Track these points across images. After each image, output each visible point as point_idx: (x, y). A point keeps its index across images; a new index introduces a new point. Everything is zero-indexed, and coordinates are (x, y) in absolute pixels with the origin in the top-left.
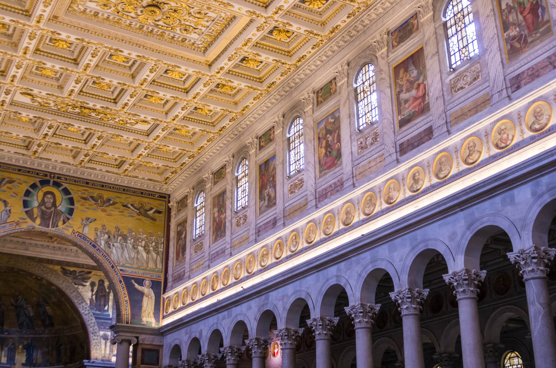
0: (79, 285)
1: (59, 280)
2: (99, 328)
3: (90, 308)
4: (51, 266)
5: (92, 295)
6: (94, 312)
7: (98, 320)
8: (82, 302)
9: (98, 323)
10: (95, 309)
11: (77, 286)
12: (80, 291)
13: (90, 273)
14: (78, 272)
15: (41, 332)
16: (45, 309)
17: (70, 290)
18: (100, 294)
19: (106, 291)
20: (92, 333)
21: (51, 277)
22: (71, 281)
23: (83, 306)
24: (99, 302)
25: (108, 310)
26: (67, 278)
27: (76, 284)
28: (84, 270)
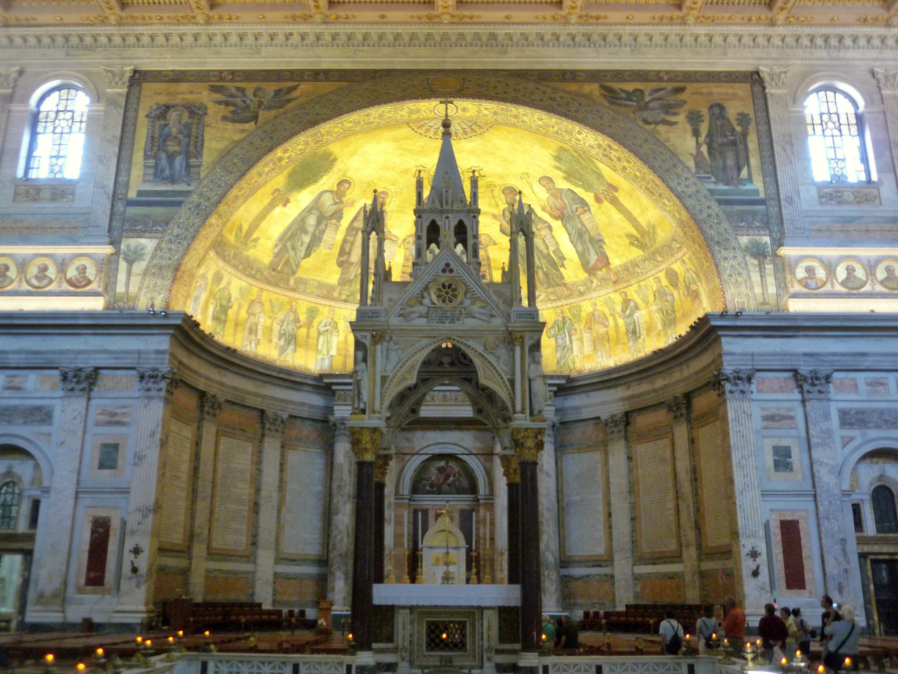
0: (657, 123)
1: (602, 118)
2: (736, 228)
3: (699, 178)
4: (573, 87)
5: (698, 145)
6: (712, 186)
7: (729, 208)
8: (675, 166)
9: (729, 216)
10: (713, 179)
11: (653, 126)
12: (662, 138)
13: (681, 90)
14: (647, 93)
15: (582, 289)
16: (581, 222)
17: (635, 138)
18: (720, 141)
19: (733, 130)
20: (718, 243)
21: (577, 111)
22: (632, 115)
23: (678, 176)
24: (720, 162)
25: (750, 179)
26: (623, 109)
27: (646, 122)
28: (663, 85)
